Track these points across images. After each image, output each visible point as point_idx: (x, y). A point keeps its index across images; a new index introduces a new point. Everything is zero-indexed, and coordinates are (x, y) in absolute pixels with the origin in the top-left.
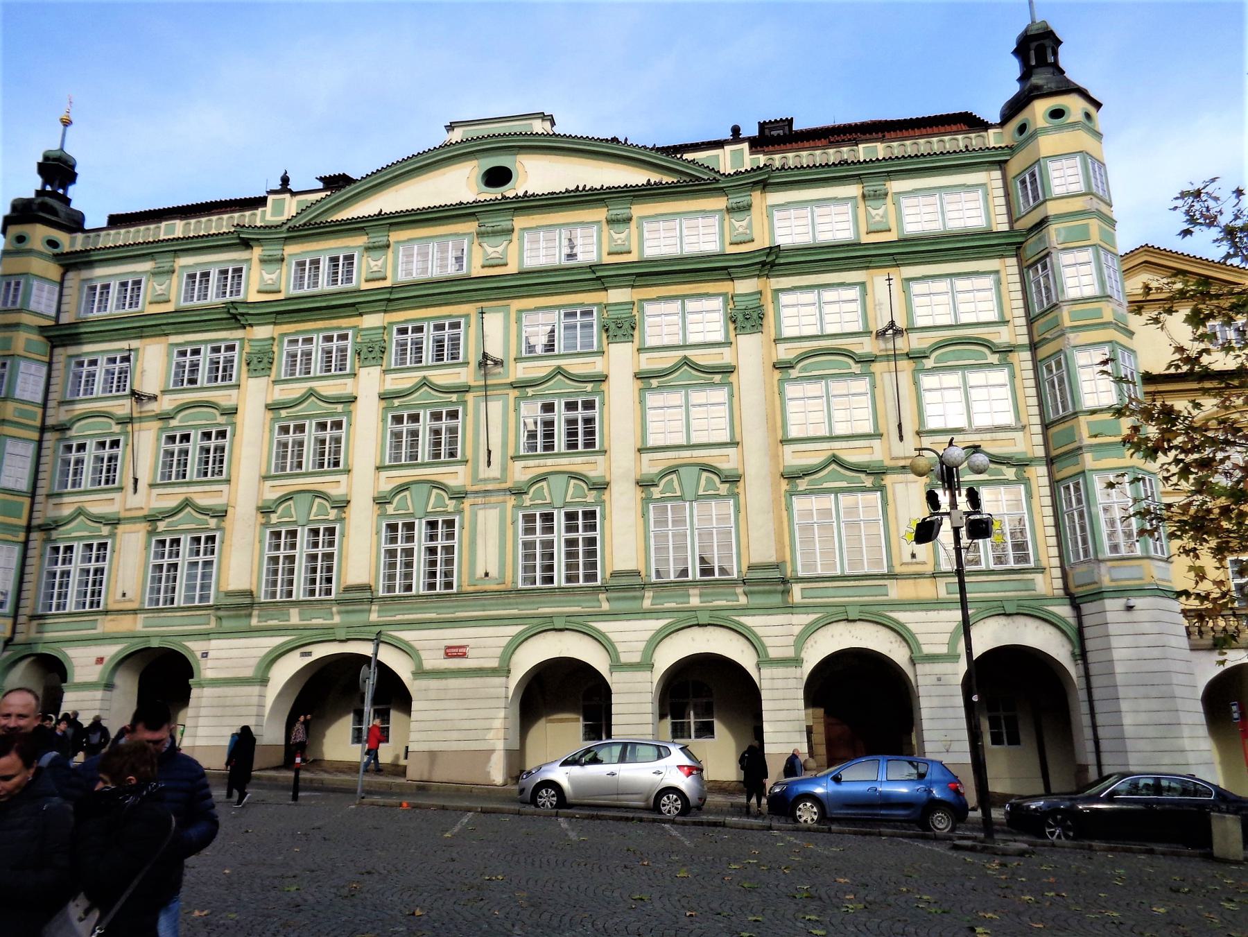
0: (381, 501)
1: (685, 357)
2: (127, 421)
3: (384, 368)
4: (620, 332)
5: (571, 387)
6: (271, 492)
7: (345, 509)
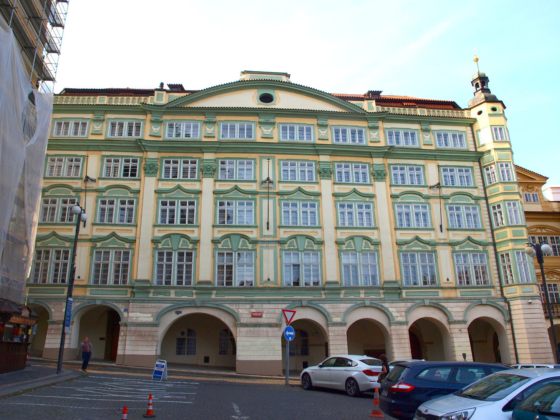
1: (355, 189)
4: (325, 175)
5: (304, 197)
6: (159, 234)
7: (197, 244)
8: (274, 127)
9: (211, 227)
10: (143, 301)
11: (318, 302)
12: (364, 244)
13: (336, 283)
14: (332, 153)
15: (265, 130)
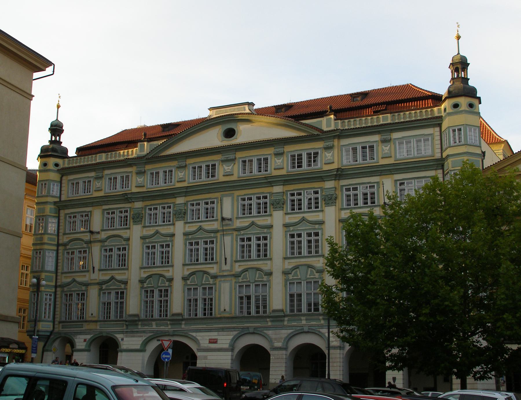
0: (185, 279)
1: (303, 217)
3: (185, 221)
5: (258, 230)
8: (235, 164)
10: (133, 332)
11: (263, 329)
12: (309, 272)
13: (282, 311)
14: (284, 183)
15: (226, 168)
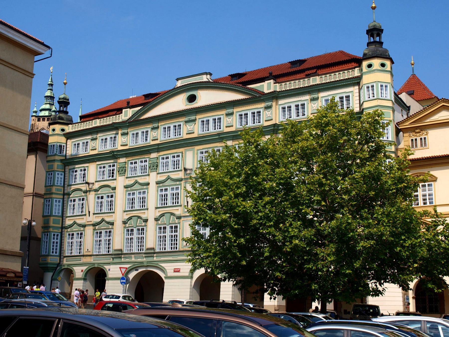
0: (157, 220)
2: (86, 192)
8: (195, 124)
9: (154, 208)
15: (189, 127)
